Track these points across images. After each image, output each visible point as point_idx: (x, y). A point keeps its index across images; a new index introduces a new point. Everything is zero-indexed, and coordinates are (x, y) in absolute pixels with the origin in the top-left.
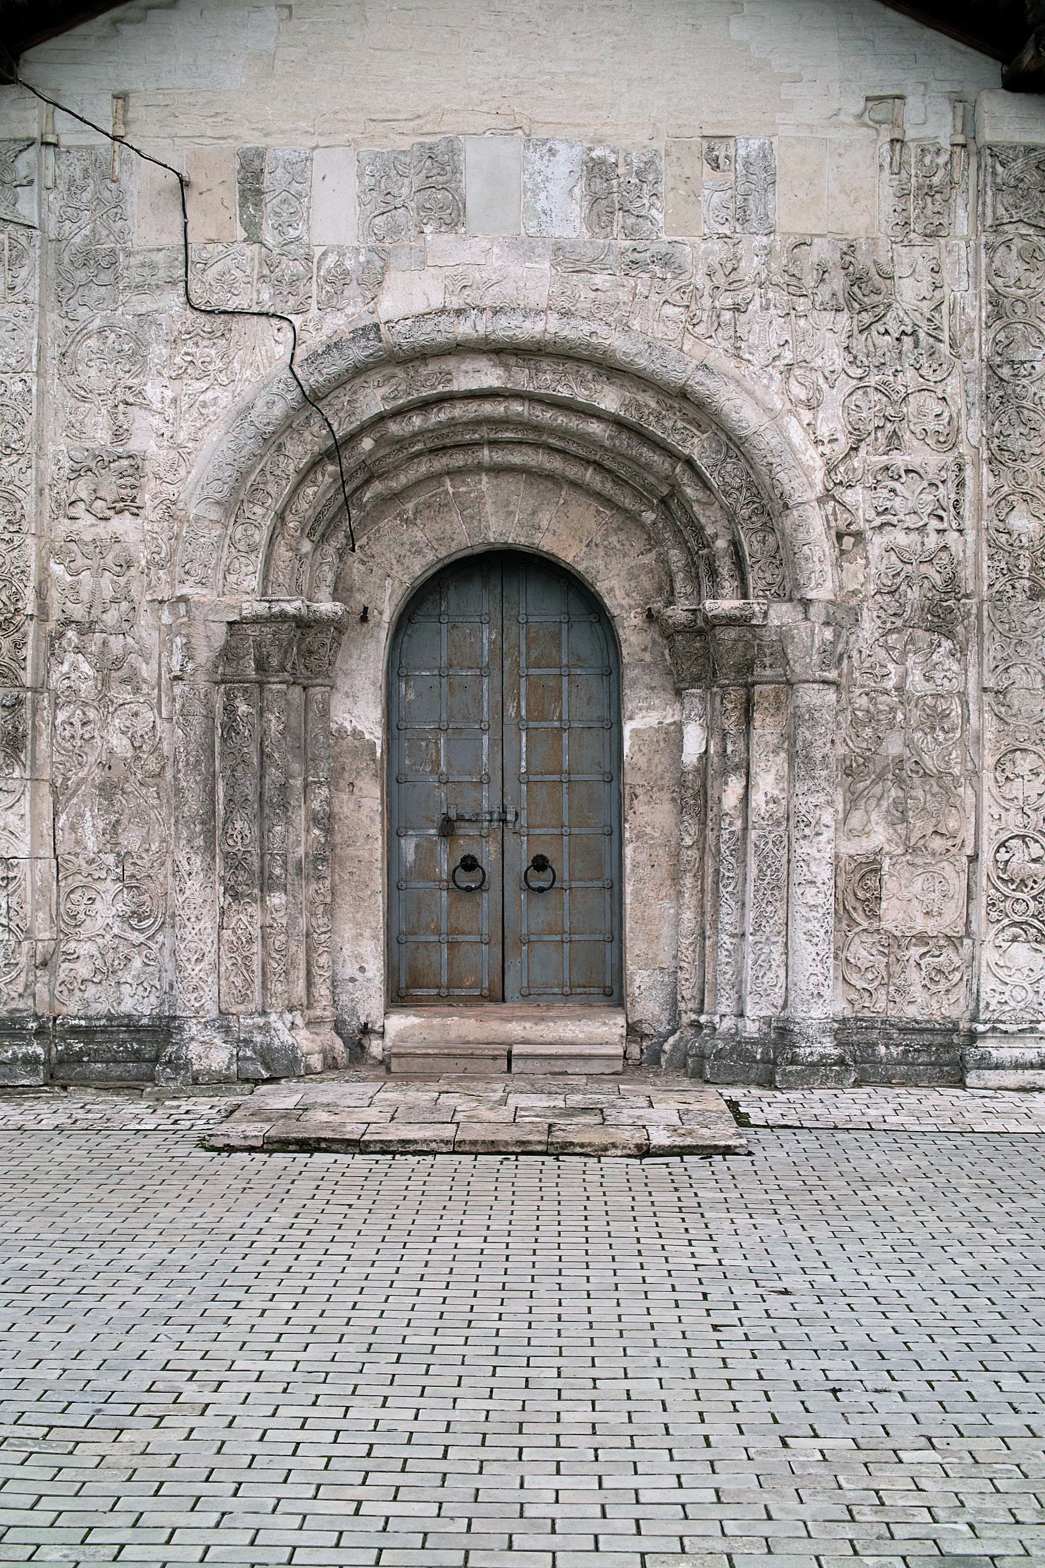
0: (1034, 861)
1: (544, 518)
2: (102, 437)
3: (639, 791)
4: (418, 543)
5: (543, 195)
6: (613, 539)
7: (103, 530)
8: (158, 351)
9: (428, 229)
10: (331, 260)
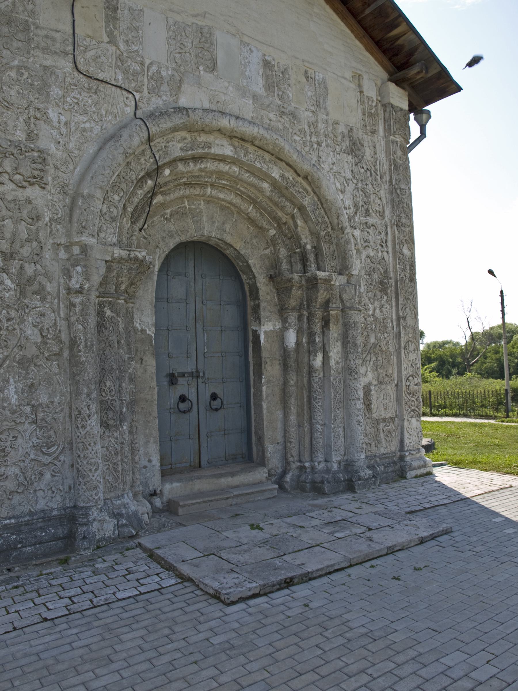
0: (416, 385)
1: (228, 227)
2: (20, 135)
3: (268, 360)
4: (172, 231)
5: (248, 69)
6: (254, 241)
7: (20, 194)
8: (56, 91)
9: (201, 68)
10: (154, 68)
